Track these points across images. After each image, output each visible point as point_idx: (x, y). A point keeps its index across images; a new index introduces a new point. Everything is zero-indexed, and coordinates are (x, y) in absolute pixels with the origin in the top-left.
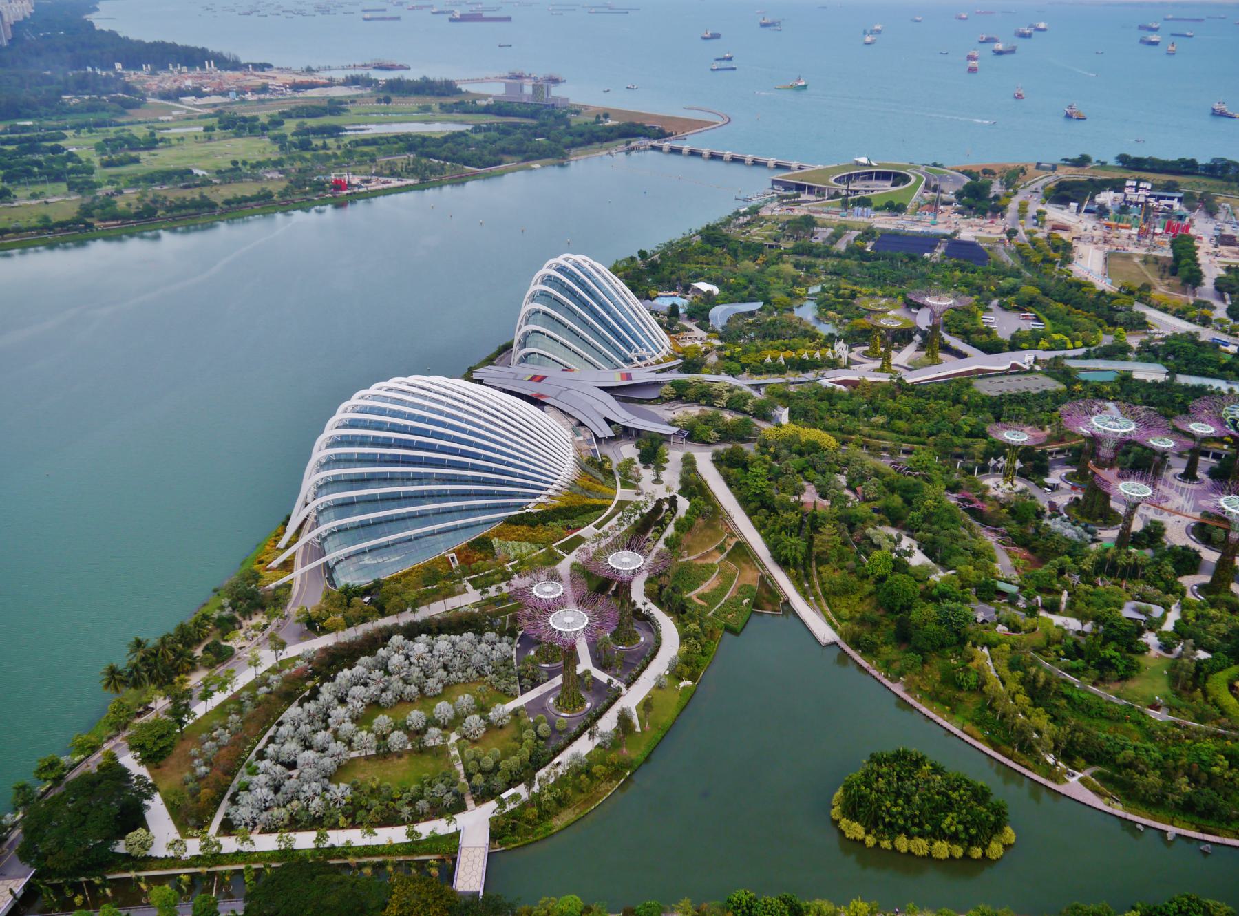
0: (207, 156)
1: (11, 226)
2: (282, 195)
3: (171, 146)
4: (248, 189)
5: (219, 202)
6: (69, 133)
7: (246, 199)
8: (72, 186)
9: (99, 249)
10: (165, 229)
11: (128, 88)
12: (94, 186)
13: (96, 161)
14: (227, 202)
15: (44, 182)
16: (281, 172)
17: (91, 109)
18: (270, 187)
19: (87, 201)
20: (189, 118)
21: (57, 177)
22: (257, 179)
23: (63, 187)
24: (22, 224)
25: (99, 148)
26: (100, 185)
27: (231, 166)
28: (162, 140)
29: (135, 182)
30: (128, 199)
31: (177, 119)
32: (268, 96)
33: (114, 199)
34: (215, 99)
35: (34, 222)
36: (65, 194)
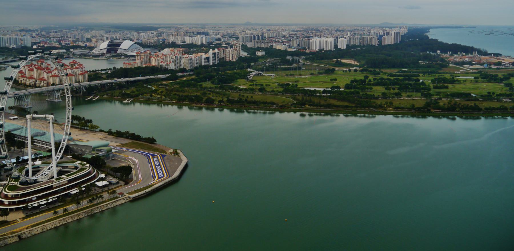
0: (475, 89)
1: (401, 106)
2: (511, 109)
3: (461, 83)
4: (496, 105)
5: (483, 108)
6: (421, 75)
7: (494, 109)
8: (423, 95)
9: (431, 120)
10: (458, 116)
11: (442, 60)
12: (431, 95)
13: (432, 86)
14: (486, 109)
15: (413, 91)
16: (510, 99)
17: (429, 66)
18: (506, 105)
19: (429, 101)
20: (467, 73)
21: (417, 90)
22: (500, 101)
23: (419, 94)
24: (404, 106)
25: (433, 81)
26: (433, 95)
27: (487, 94)
28: (457, 80)
29: (447, 96)
30: (444, 101)
31: (462, 73)
32: (501, 67)
33: (438, 101)
34: (478, 66)
35: (408, 106)
36: (420, 97)
